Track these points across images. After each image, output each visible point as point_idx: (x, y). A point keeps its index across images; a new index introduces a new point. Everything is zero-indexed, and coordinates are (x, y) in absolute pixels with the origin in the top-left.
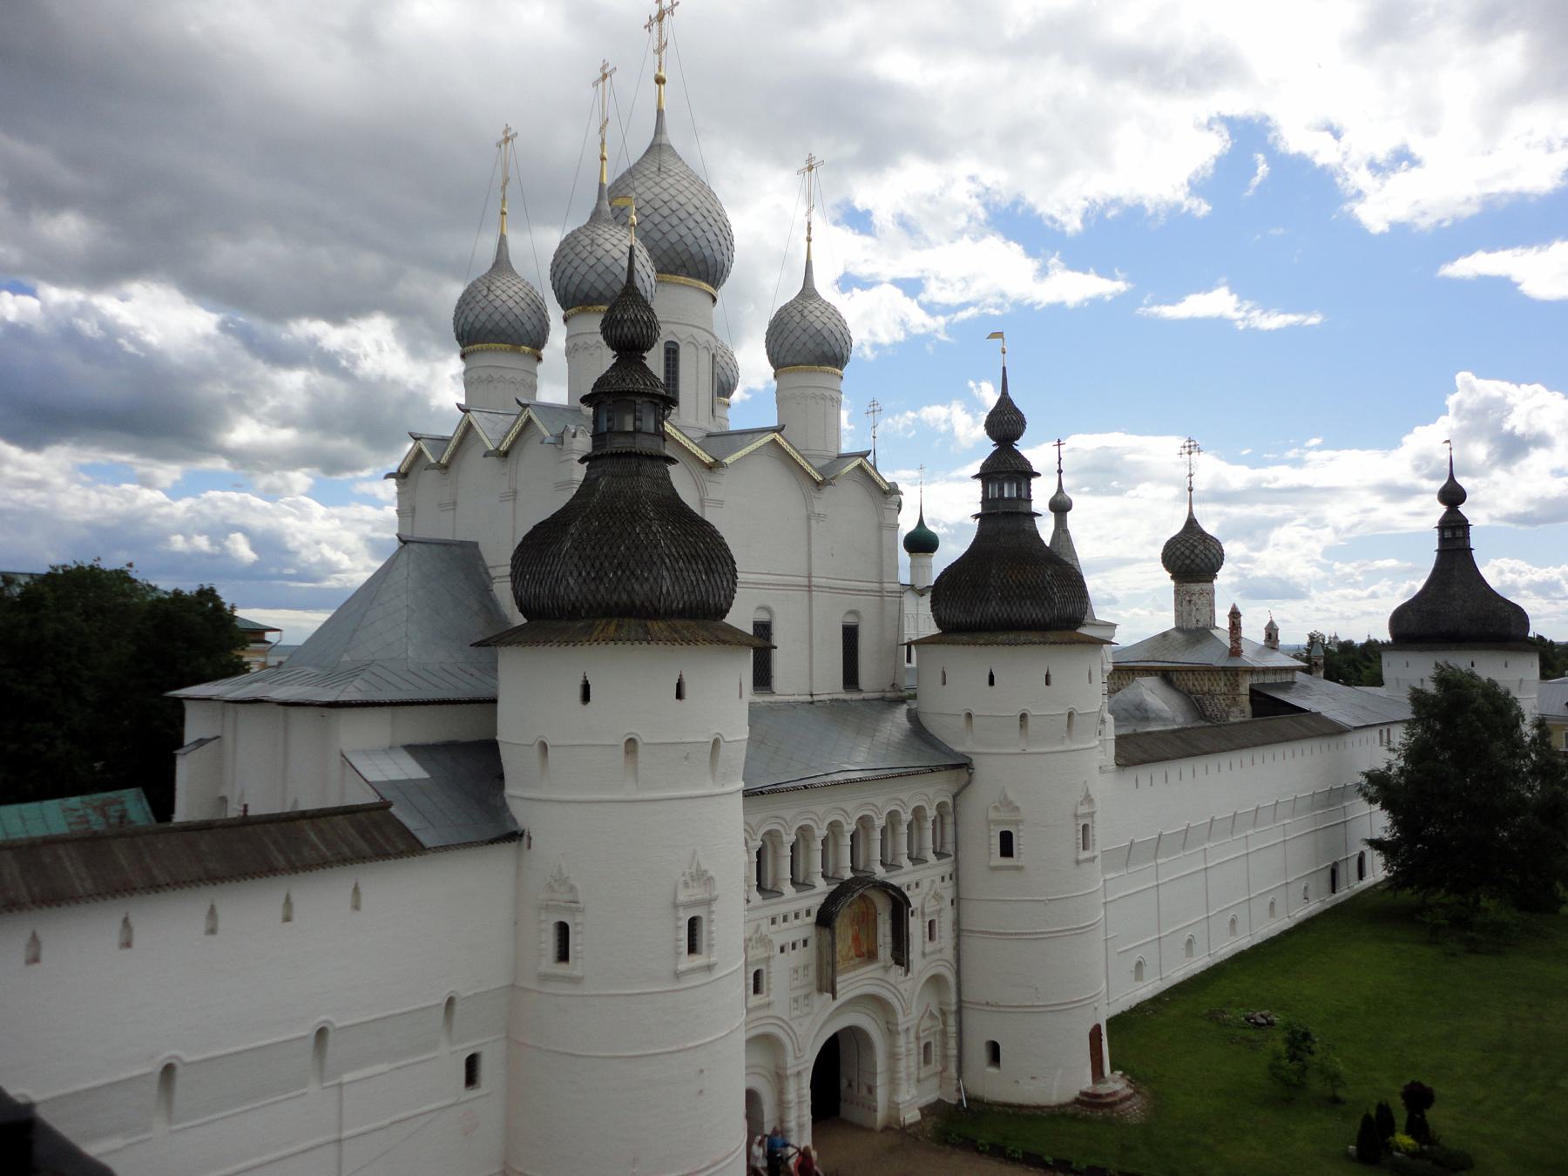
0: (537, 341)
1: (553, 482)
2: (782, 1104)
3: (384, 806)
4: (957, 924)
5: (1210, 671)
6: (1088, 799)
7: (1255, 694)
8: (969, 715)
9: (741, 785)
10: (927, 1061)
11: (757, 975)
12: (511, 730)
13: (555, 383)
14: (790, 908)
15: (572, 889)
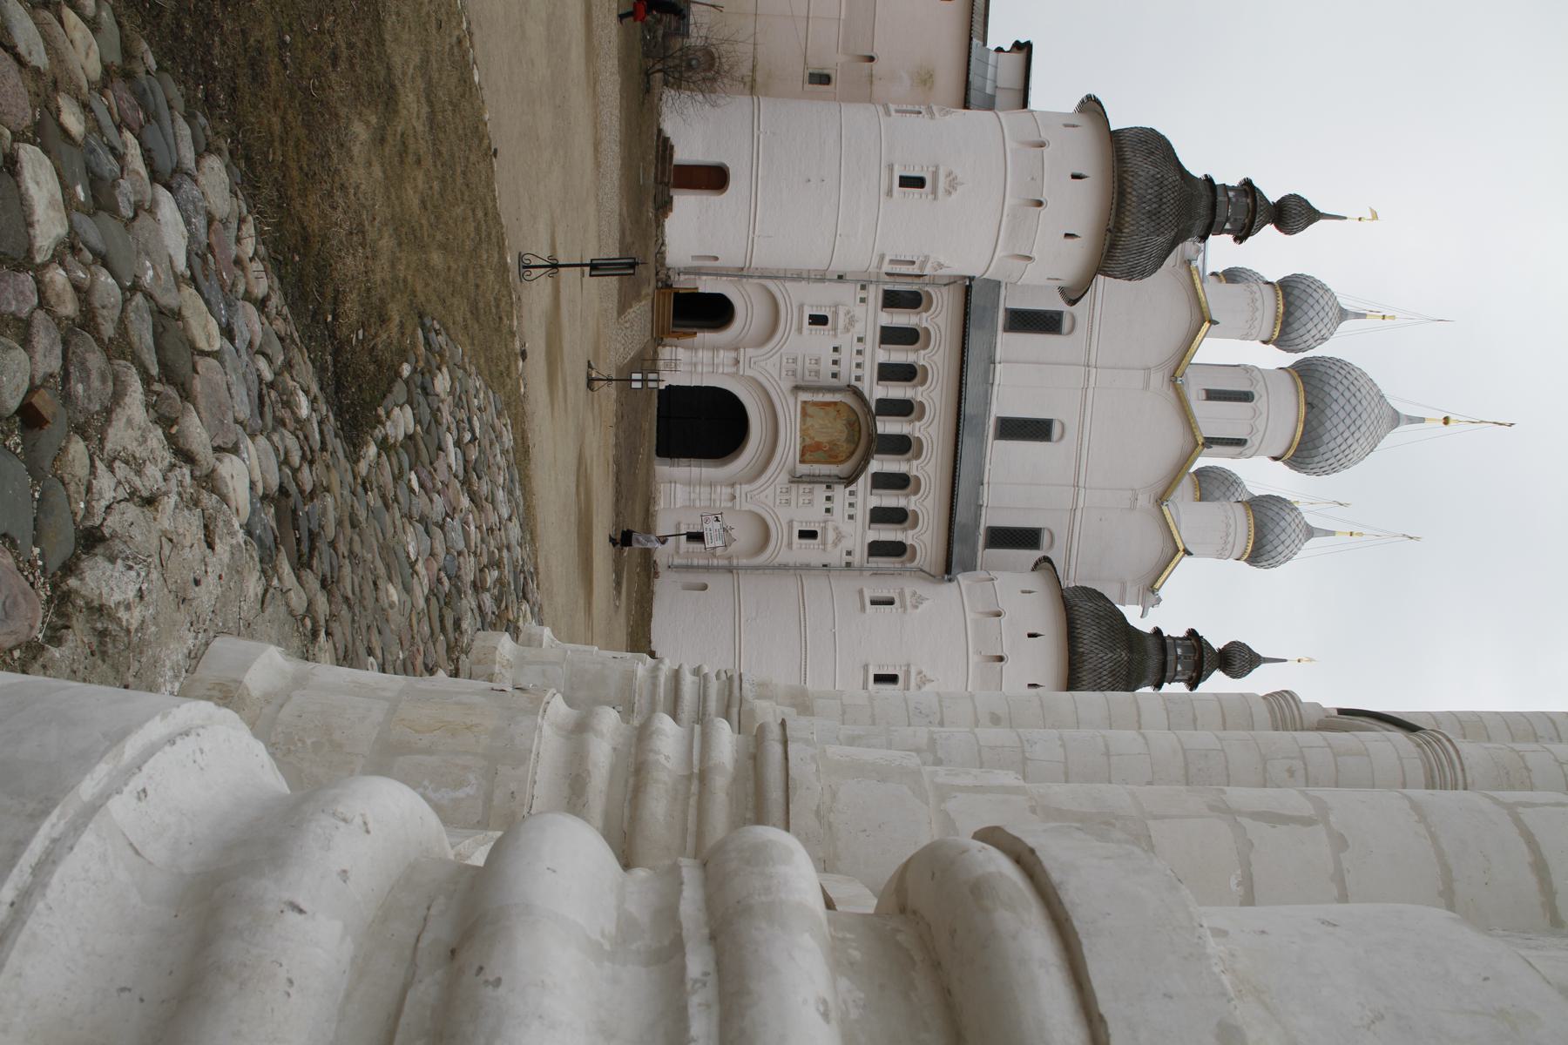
2: (715, 348)
14: (866, 359)
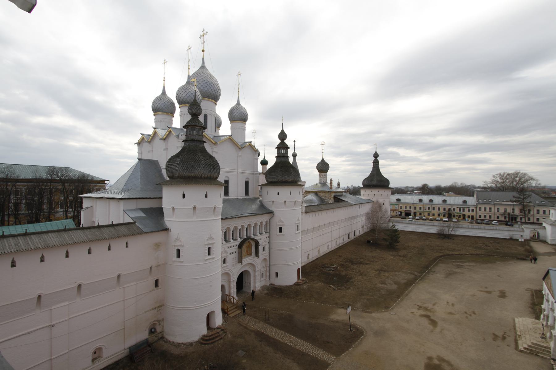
0: (172, 112)
1: (176, 146)
2: (230, 288)
3: (134, 223)
4: (270, 247)
5: (326, 192)
6: (298, 220)
7: (335, 197)
9: (221, 217)
10: (262, 276)
11: (224, 260)
12: (166, 205)
13: (177, 122)
14: (232, 245)
15: (180, 241)
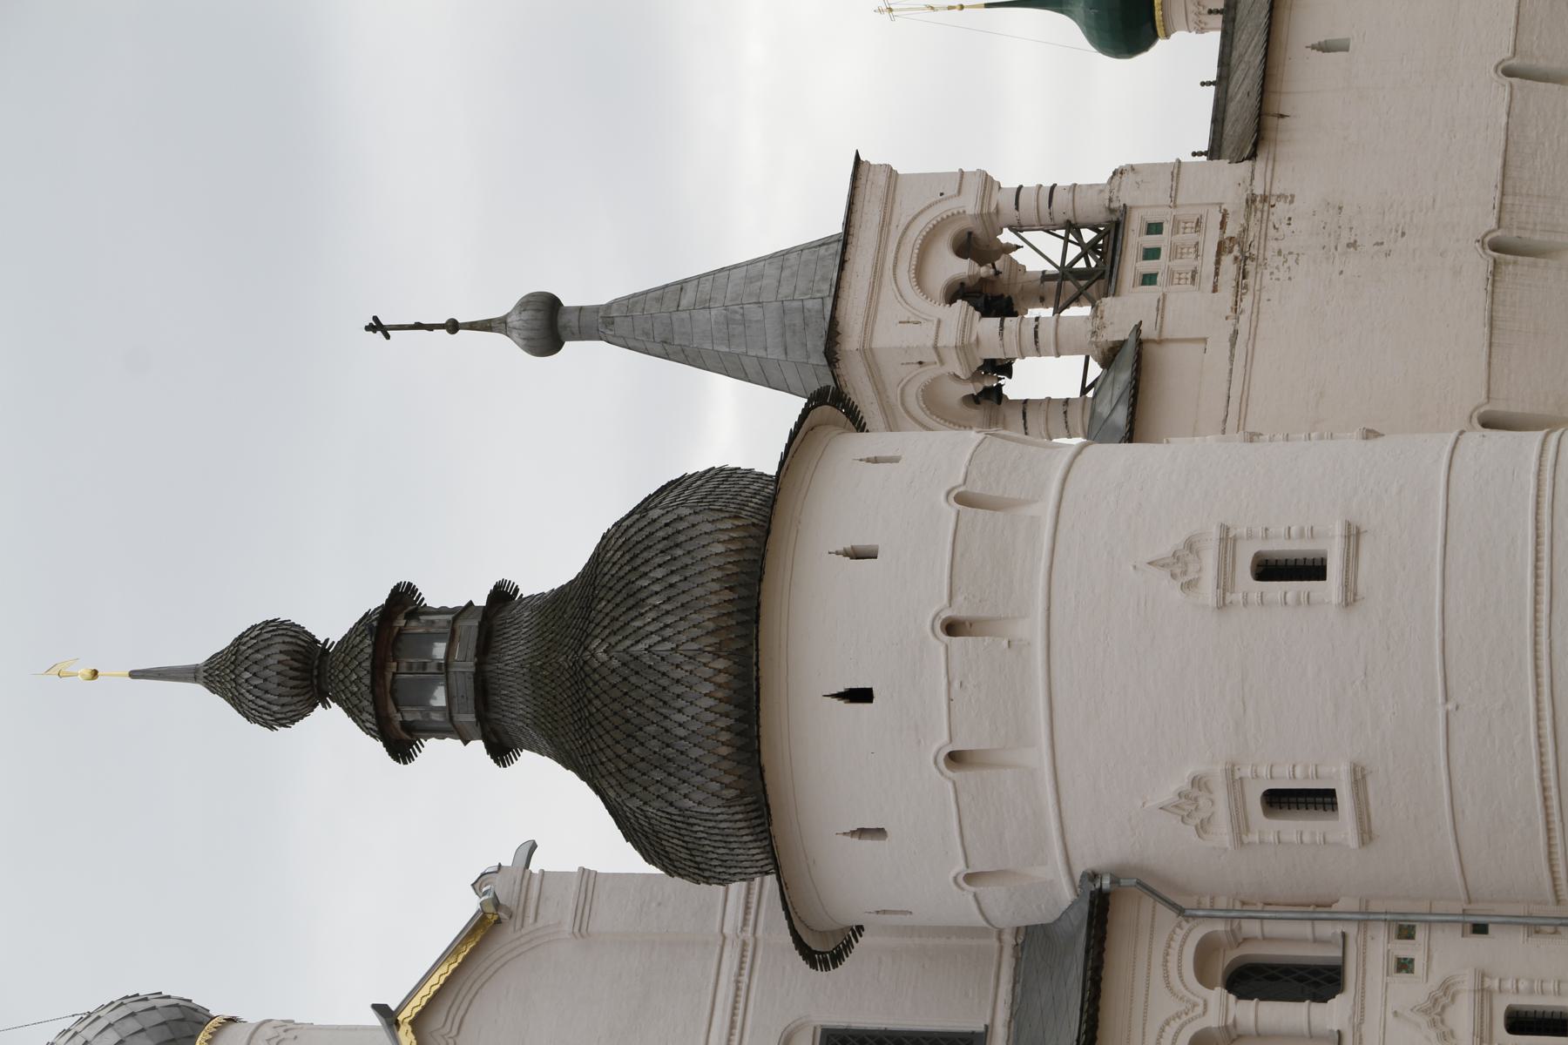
6: (1179, 563)
8: (970, 878)
